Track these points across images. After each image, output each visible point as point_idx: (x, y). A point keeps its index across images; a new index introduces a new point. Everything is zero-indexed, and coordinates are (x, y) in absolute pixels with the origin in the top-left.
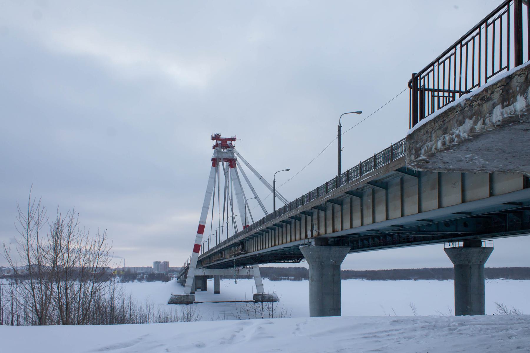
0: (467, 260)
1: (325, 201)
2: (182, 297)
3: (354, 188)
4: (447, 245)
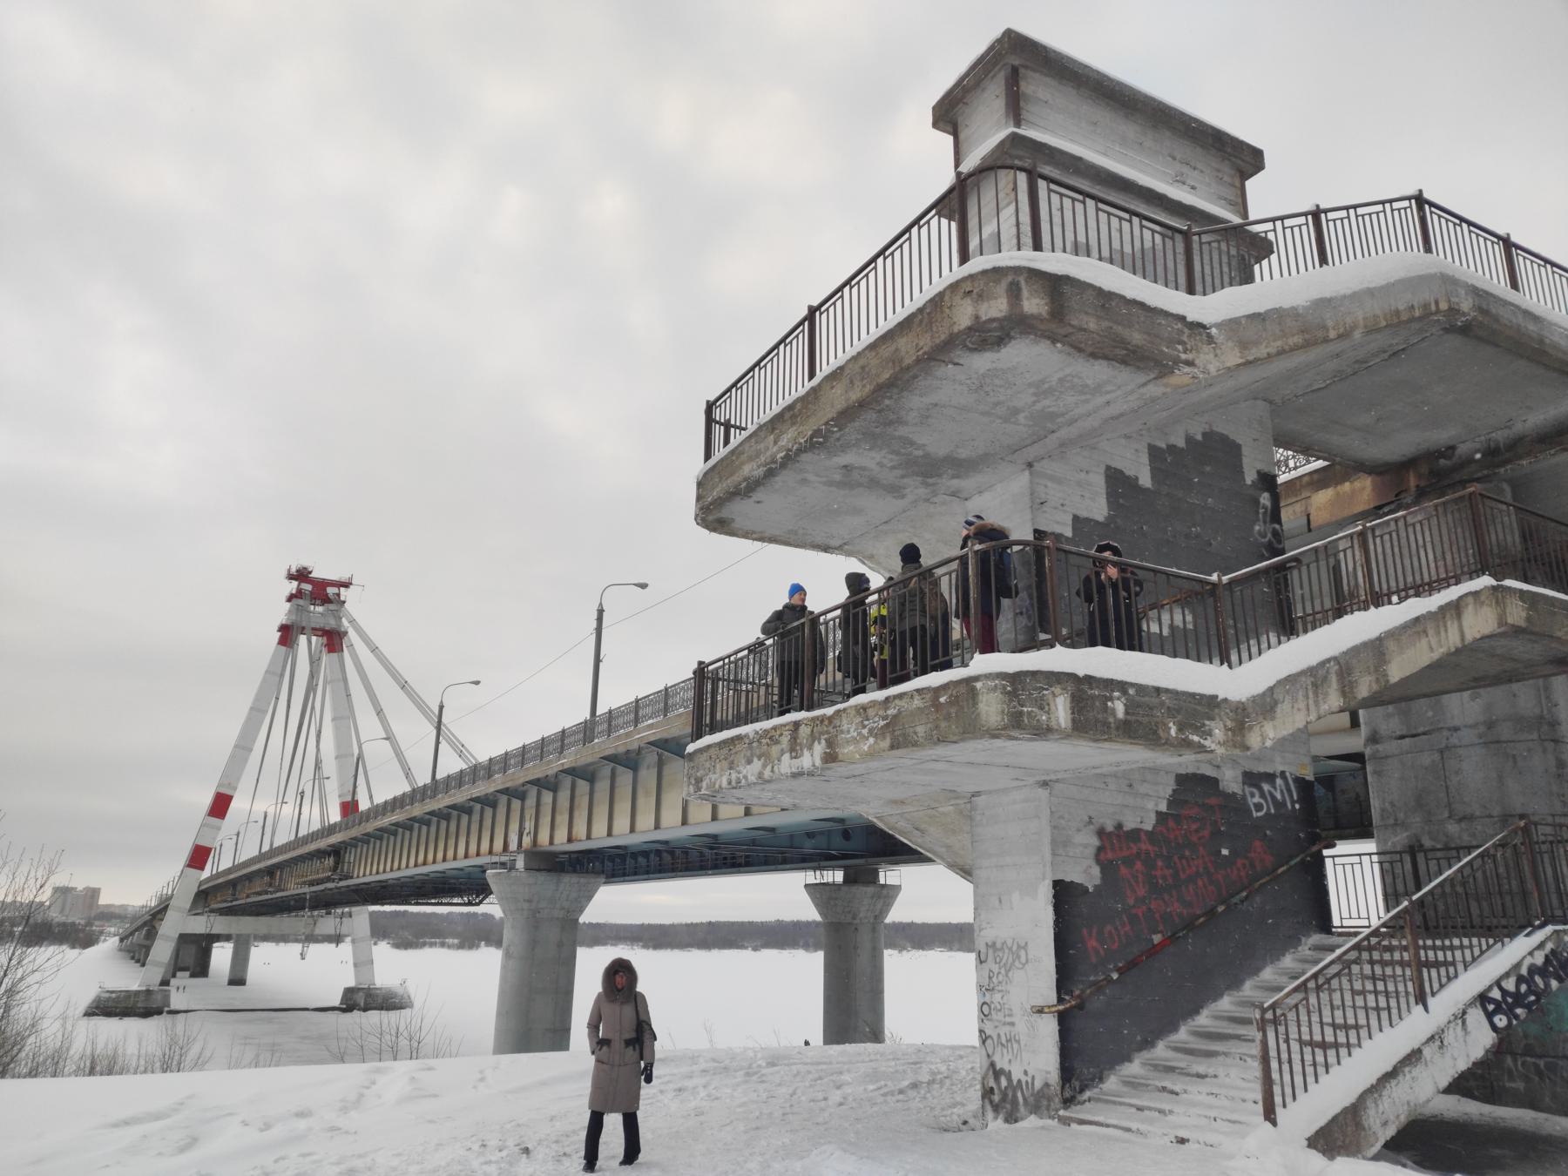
0: (850, 912)
1: (556, 770)
3: (622, 750)
4: (811, 877)
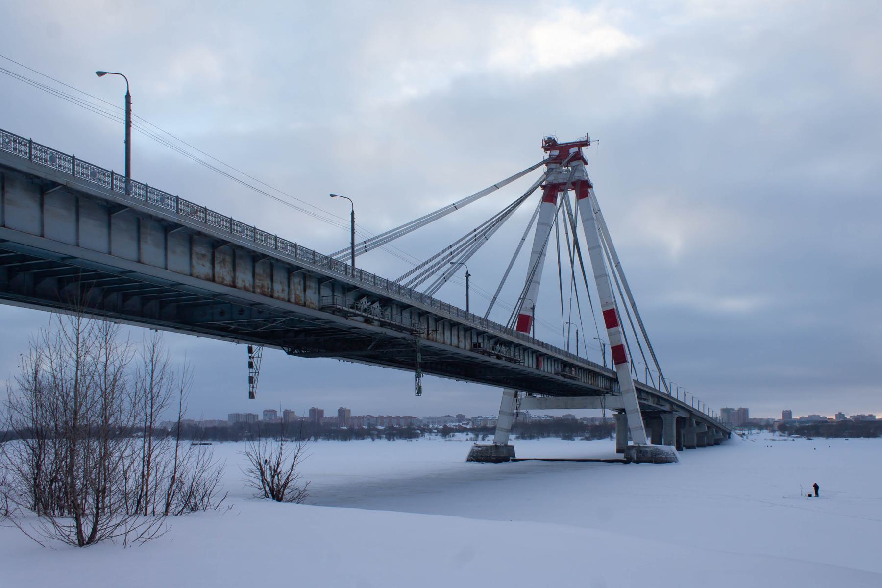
2: (489, 449)
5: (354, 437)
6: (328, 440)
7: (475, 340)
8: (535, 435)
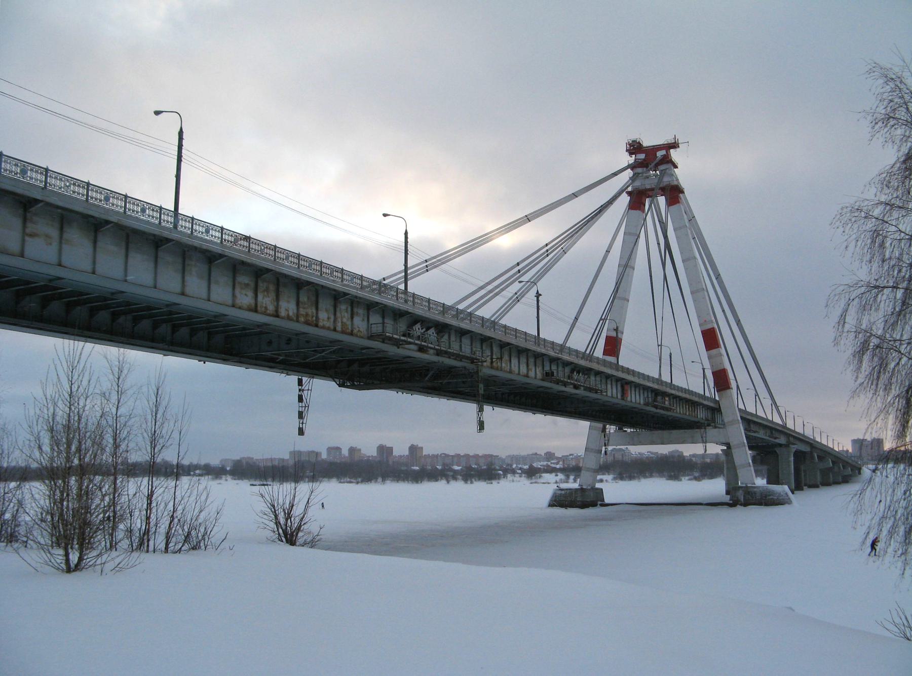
2: (574, 493)
5: (426, 478)
6: (398, 481)
7: (547, 368)
8: (635, 475)
